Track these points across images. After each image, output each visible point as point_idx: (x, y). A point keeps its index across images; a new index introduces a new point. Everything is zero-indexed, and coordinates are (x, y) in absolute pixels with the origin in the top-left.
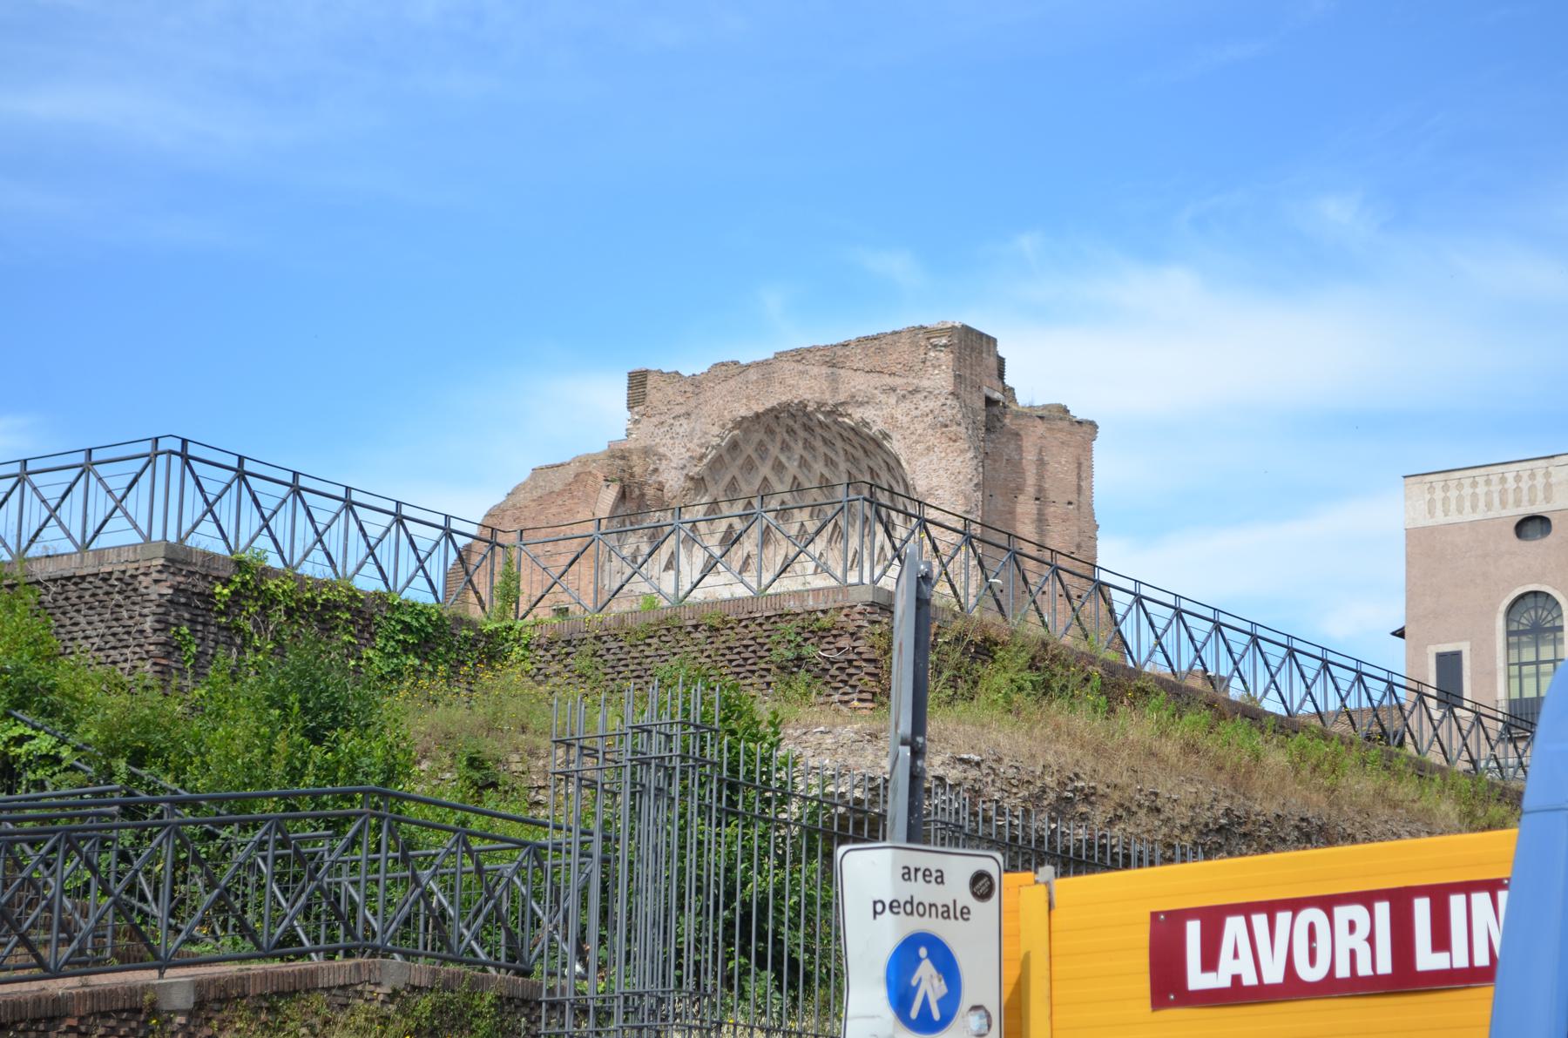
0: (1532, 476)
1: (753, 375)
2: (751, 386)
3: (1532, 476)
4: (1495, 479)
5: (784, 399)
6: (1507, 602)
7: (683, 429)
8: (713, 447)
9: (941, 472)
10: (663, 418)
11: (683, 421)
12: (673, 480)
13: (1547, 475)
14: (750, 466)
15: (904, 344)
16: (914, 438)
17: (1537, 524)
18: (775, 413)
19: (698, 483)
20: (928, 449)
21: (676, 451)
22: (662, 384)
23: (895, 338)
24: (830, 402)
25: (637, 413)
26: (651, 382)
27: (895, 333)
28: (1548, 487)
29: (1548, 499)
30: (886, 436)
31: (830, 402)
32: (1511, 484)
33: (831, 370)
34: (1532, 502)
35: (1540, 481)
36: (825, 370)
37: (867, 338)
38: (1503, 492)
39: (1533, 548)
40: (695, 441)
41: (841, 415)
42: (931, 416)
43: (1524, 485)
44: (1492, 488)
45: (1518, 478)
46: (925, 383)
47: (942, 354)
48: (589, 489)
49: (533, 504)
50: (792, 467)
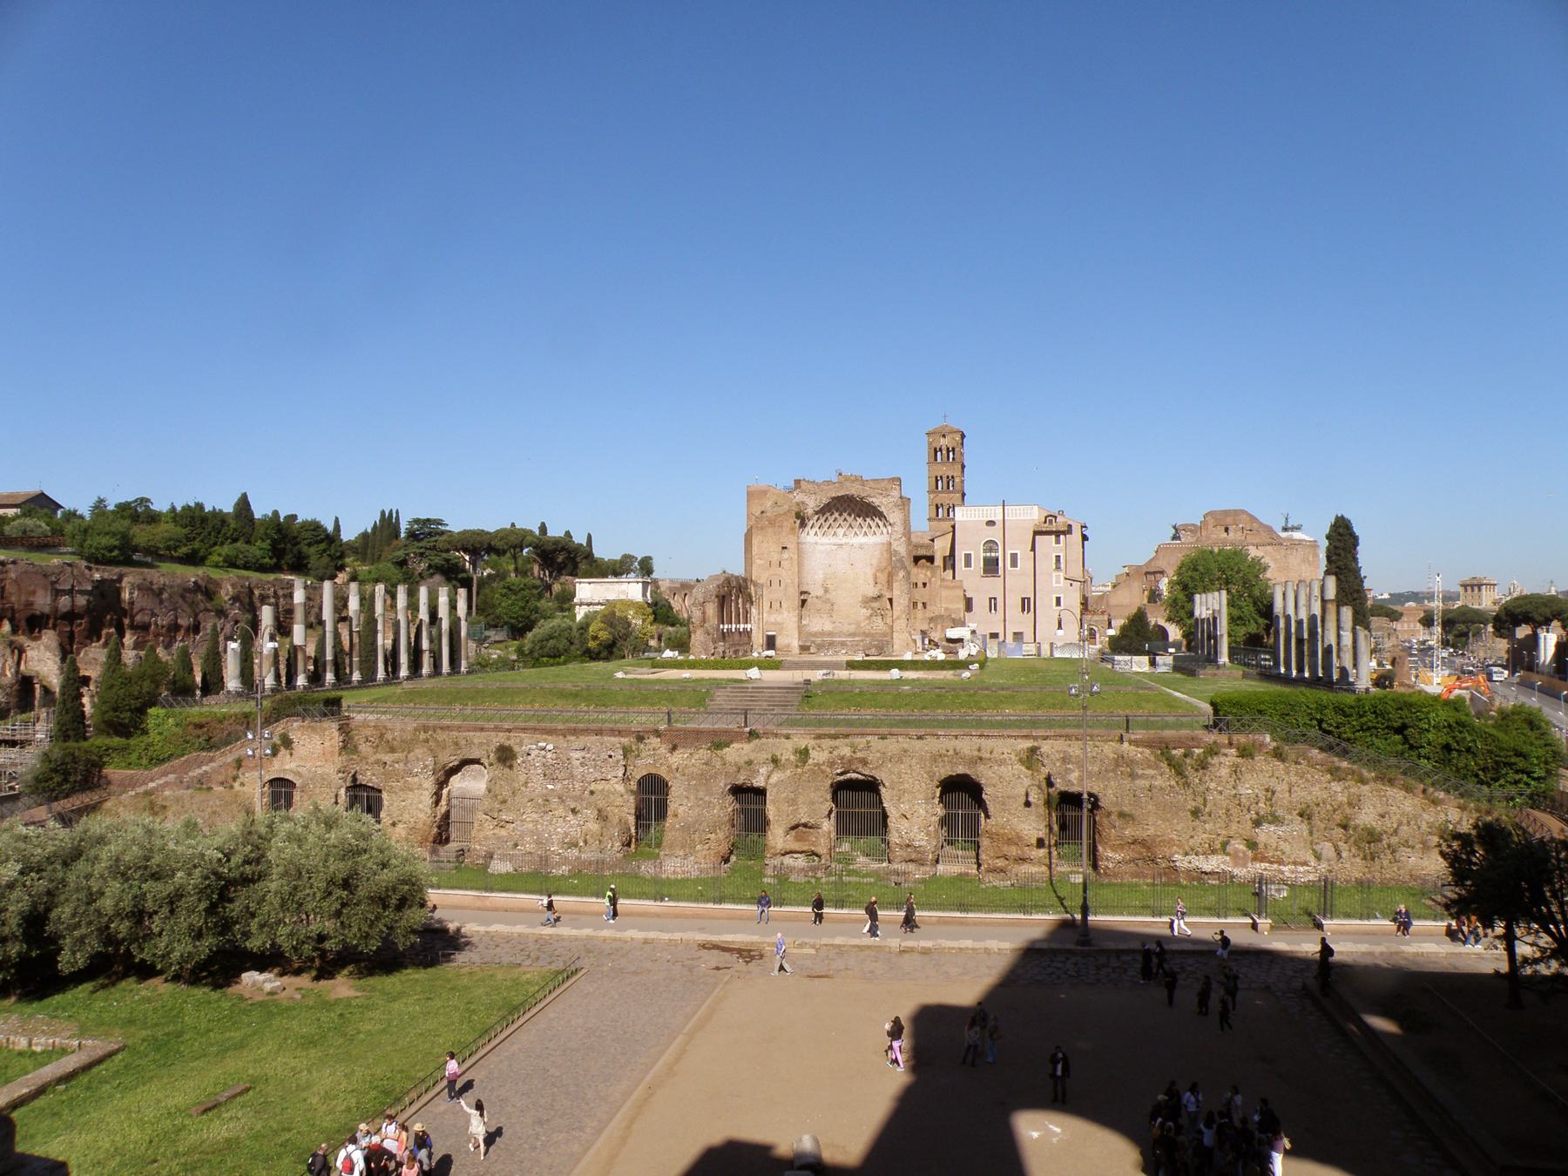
12: (810, 511)
18: (843, 497)
19: (817, 513)
26: (802, 483)
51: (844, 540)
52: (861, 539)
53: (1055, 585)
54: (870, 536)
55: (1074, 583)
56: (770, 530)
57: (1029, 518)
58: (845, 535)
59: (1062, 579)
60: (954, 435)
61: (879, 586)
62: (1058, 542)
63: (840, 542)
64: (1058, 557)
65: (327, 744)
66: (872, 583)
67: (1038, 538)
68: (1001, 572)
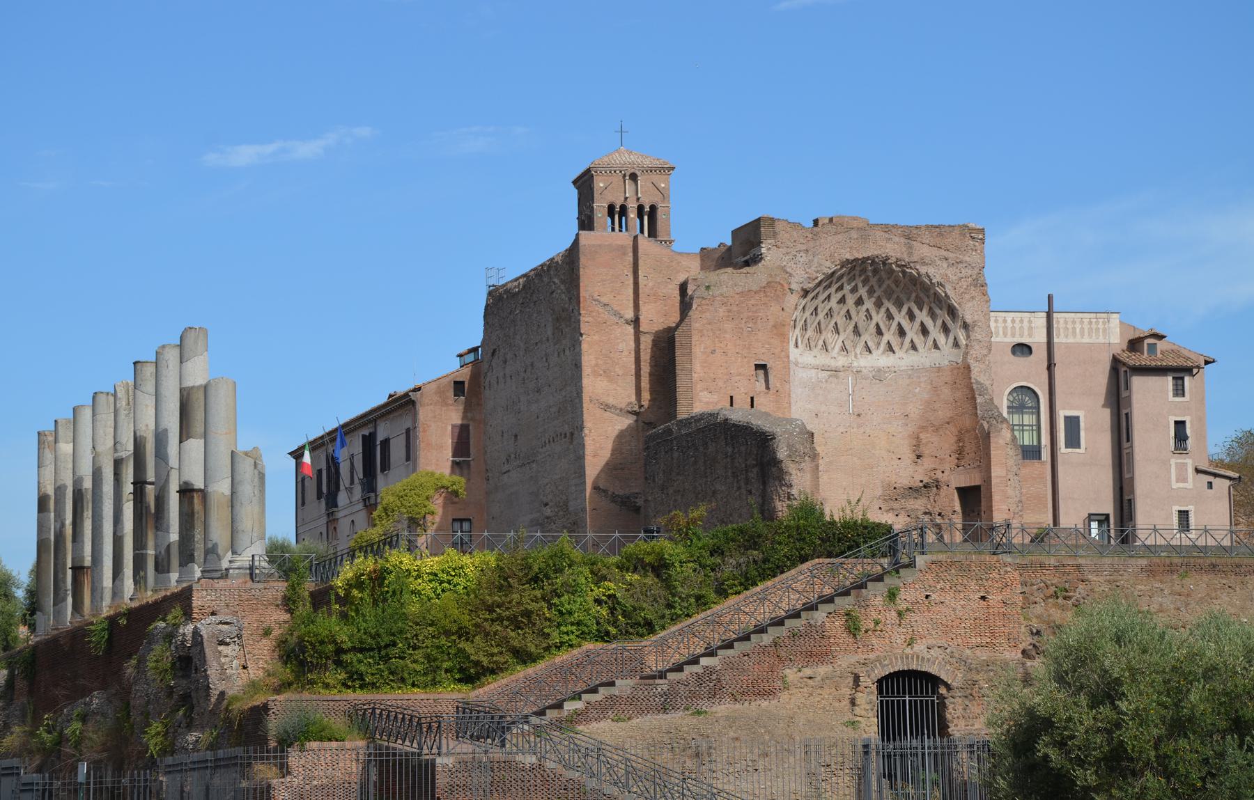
0: (1022, 321)
1: (854, 235)
2: (853, 241)
3: (1022, 321)
4: (1000, 320)
5: (876, 253)
6: (1009, 390)
7: (801, 260)
8: (824, 274)
9: (980, 313)
10: (789, 250)
11: (802, 254)
13: (1030, 322)
14: (829, 286)
15: (957, 231)
16: (962, 290)
17: (1026, 349)
18: (865, 260)
20: (973, 298)
21: (798, 272)
22: (789, 229)
23: (951, 229)
24: (907, 260)
25: (770, 244)
26: (779, 227)
27: (950, 226)
28: (1030, 328)
29: (1030, 335)
30: (940, 284)
31: (907, 260)
32: (1009, 324)
33: (907, 241)
34: (1021, 335)
35: (1026, 324)
36: (902, 240)
37: (932, 226)
38: (1005, 328)
39: (1021, 361)
40: (813, 268)
41: (911, 268)
42: (970, 279)
43: (1017, 325)
44: (999, 325)
45: (1013, 321)
46: (967, 259)
47: (977, 244)
48: (778, 292)
49: (737, 296)
50: (847, 288)
51: (842, 361)
52: (879, 359)
53: (1175, 485)
54: (899, 353)
55: (1217, 482)
56: (728, 326)
57: (1101, 340)
58: (844, 348)
59: (1190, 470)
60: (655, 177)
61: (927, 463)
62: (1179, 391)
63: (833, 364)
64: (1180, 425)
65: (995, 598)
66: (908, 456)
67: (1137, 382)
68: (1046, 455)
